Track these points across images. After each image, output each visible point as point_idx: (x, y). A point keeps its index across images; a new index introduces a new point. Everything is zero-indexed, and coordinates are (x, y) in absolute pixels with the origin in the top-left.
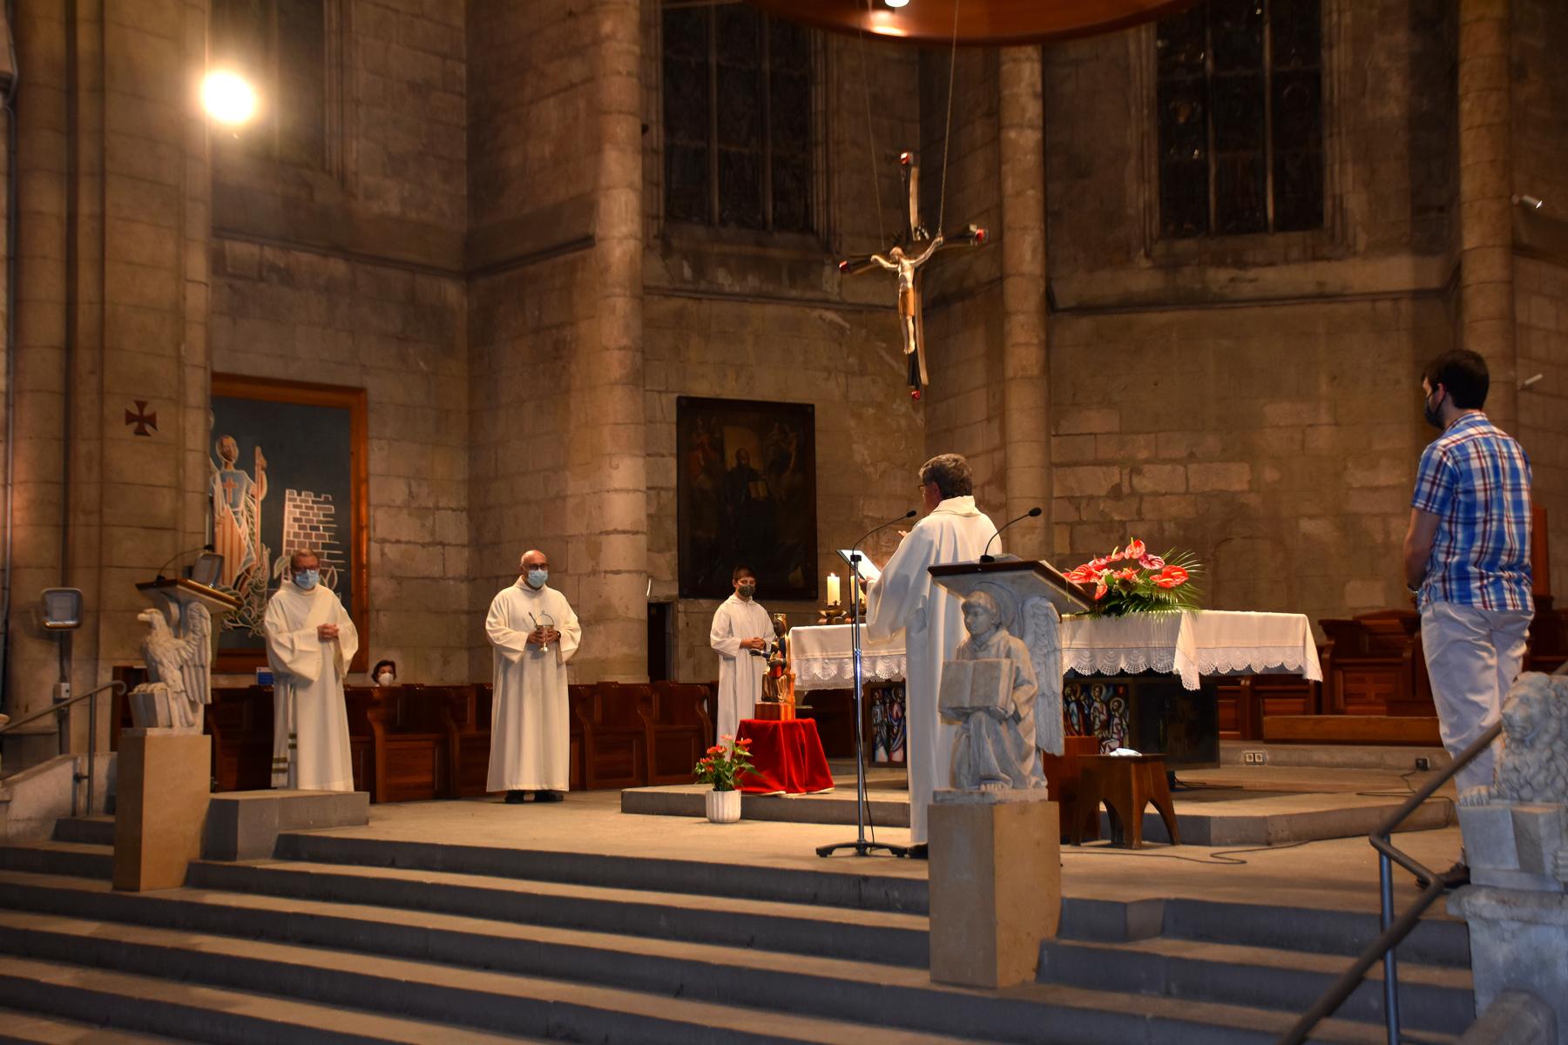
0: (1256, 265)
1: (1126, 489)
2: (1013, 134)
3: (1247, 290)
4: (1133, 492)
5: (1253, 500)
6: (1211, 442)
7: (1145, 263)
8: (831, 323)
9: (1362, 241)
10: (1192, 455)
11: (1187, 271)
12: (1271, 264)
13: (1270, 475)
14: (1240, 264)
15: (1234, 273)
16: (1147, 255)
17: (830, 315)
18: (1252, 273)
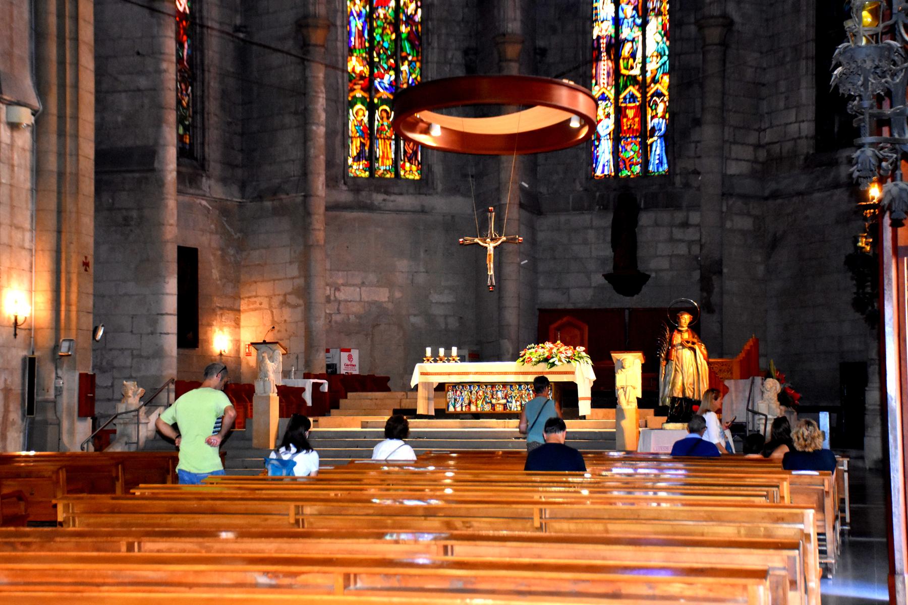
0: (395, 194)
1: (332, 298)
2: (314, 128)
3: (390, 205)
4: (336, 300)
5: (390, 306)
6: (372, 277)
7: (344, 188)
8: (205, 206)
9: (440, 187)
10: (363, 283)
11: (364, 193)
12: (401, 194)
13: (398, 295)
14: (387, 193)
15: (385, 197)
16: (345, 184)
17: (204, 203)
18: (392, 198)
